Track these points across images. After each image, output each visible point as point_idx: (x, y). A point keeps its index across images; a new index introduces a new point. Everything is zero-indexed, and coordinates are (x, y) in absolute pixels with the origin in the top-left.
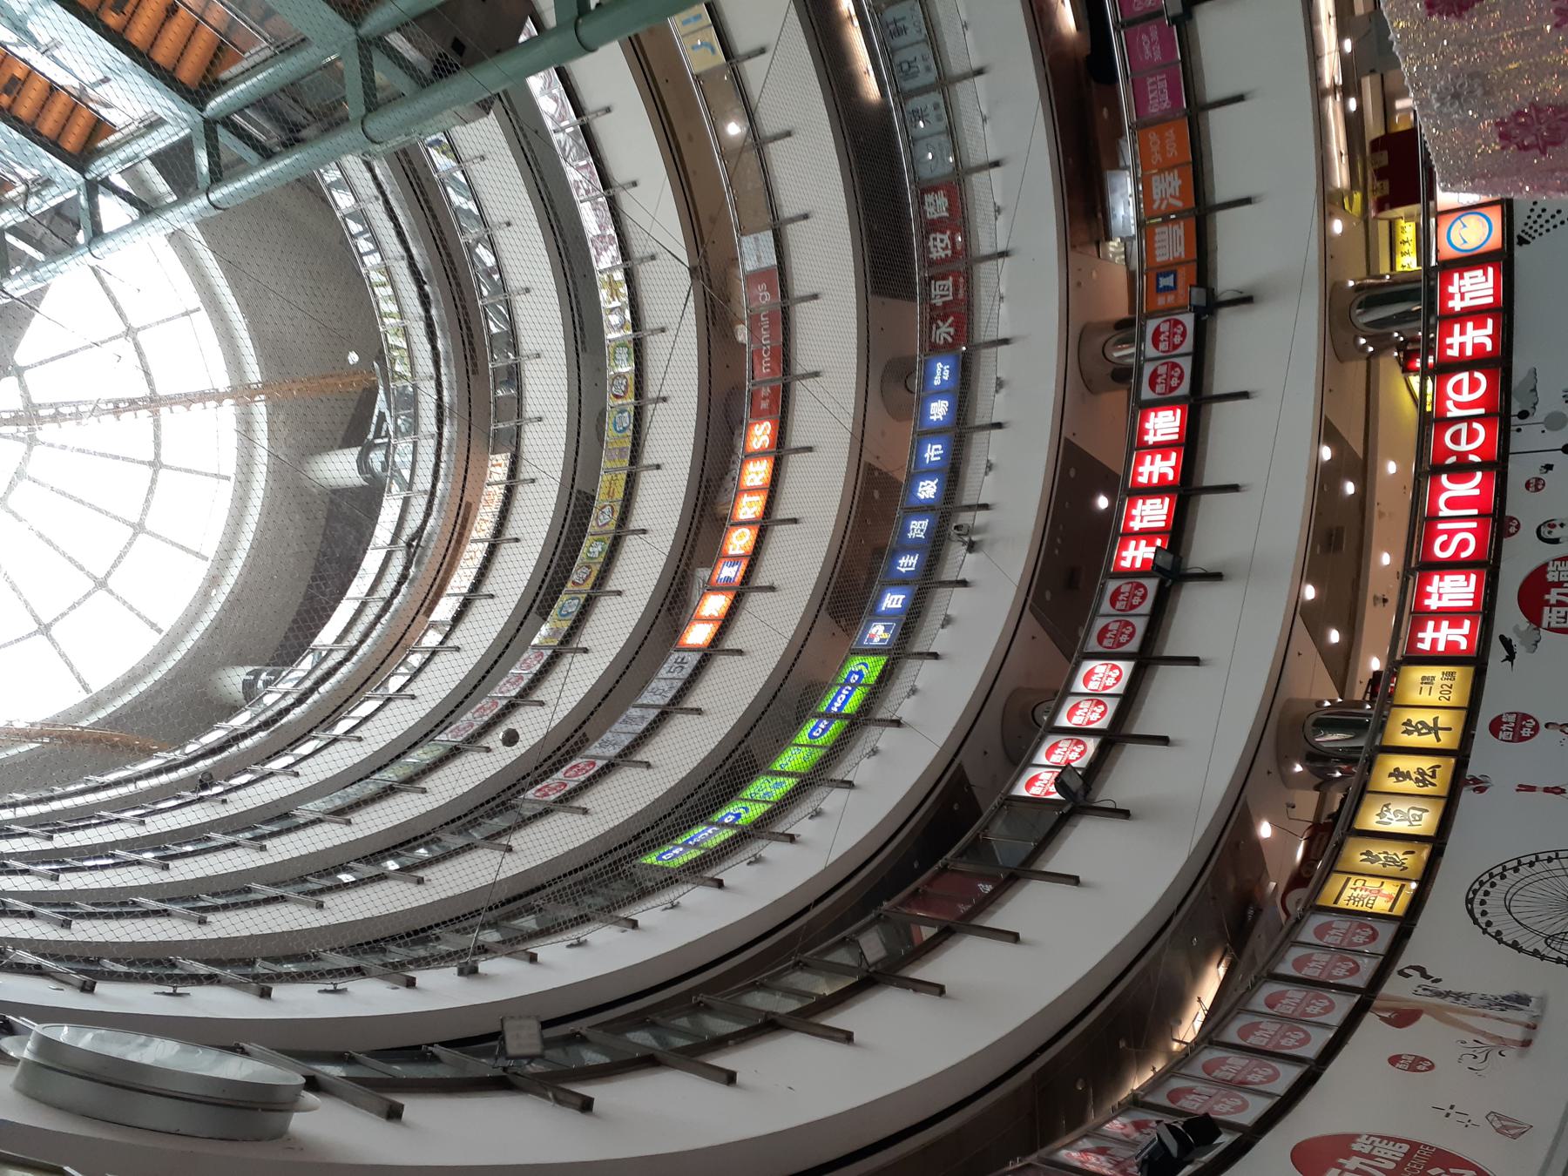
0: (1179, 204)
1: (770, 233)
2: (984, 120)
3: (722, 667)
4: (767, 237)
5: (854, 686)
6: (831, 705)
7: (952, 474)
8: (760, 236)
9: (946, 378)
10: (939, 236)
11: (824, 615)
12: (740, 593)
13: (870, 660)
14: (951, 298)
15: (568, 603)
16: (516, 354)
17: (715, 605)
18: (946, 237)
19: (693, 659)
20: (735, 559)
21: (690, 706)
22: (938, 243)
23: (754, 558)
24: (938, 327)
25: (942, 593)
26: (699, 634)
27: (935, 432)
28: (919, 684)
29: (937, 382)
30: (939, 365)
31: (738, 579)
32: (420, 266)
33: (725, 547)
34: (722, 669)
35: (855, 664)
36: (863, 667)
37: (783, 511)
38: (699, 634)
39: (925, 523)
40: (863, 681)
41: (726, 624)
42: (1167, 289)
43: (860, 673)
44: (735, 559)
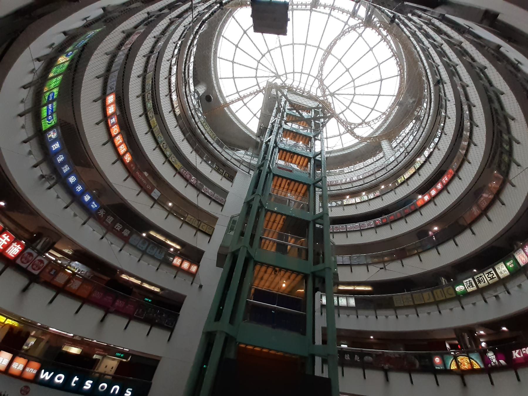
0: (68, 286)
1: (156, 199)
2: (130, 255)
3: (98, 93)
4: (156, 198)
5: (48, 115)
6: (52, 106)
7: (69, 189)
8: (157, 197)
9: (92, 205)
10: (120, 228)
11: (72, 122)
12: (106, 117)
13: (49, 126)
14: (107, 220)
15: (148, 87)
16: (204, 160)
17: (111, 110)
18: (119, 229)
19: (108, 92)
20: (113, 124)
21: (101, 78)
22: (119, 227)
23: (108, 129)
24: (104, 212)
25: (40, 158)
26: (111, 99)
27: (83, 193)
28: (23, 130)
29: (93, 203)
30: (96, 206)
31: (109, 121)
32: (210, 144)
33: (118, 126)
34: (97, 93)
35: (53, 122)
36: (50, 122)
37: (109, 145)
38: (111, 99)
39: (65, 171)
40: (46, 119)
41: (104, 107)
42: (51, 270)
43: (49, 120)
44: (113, 124)
